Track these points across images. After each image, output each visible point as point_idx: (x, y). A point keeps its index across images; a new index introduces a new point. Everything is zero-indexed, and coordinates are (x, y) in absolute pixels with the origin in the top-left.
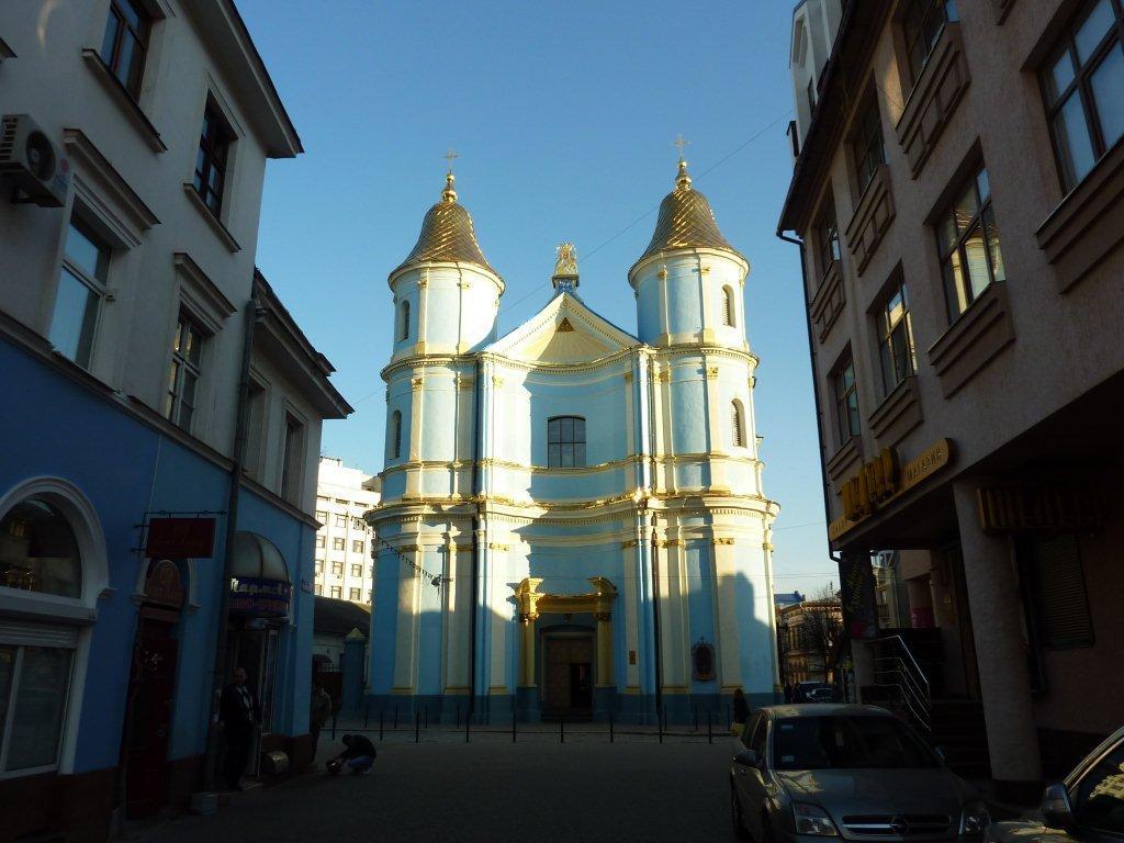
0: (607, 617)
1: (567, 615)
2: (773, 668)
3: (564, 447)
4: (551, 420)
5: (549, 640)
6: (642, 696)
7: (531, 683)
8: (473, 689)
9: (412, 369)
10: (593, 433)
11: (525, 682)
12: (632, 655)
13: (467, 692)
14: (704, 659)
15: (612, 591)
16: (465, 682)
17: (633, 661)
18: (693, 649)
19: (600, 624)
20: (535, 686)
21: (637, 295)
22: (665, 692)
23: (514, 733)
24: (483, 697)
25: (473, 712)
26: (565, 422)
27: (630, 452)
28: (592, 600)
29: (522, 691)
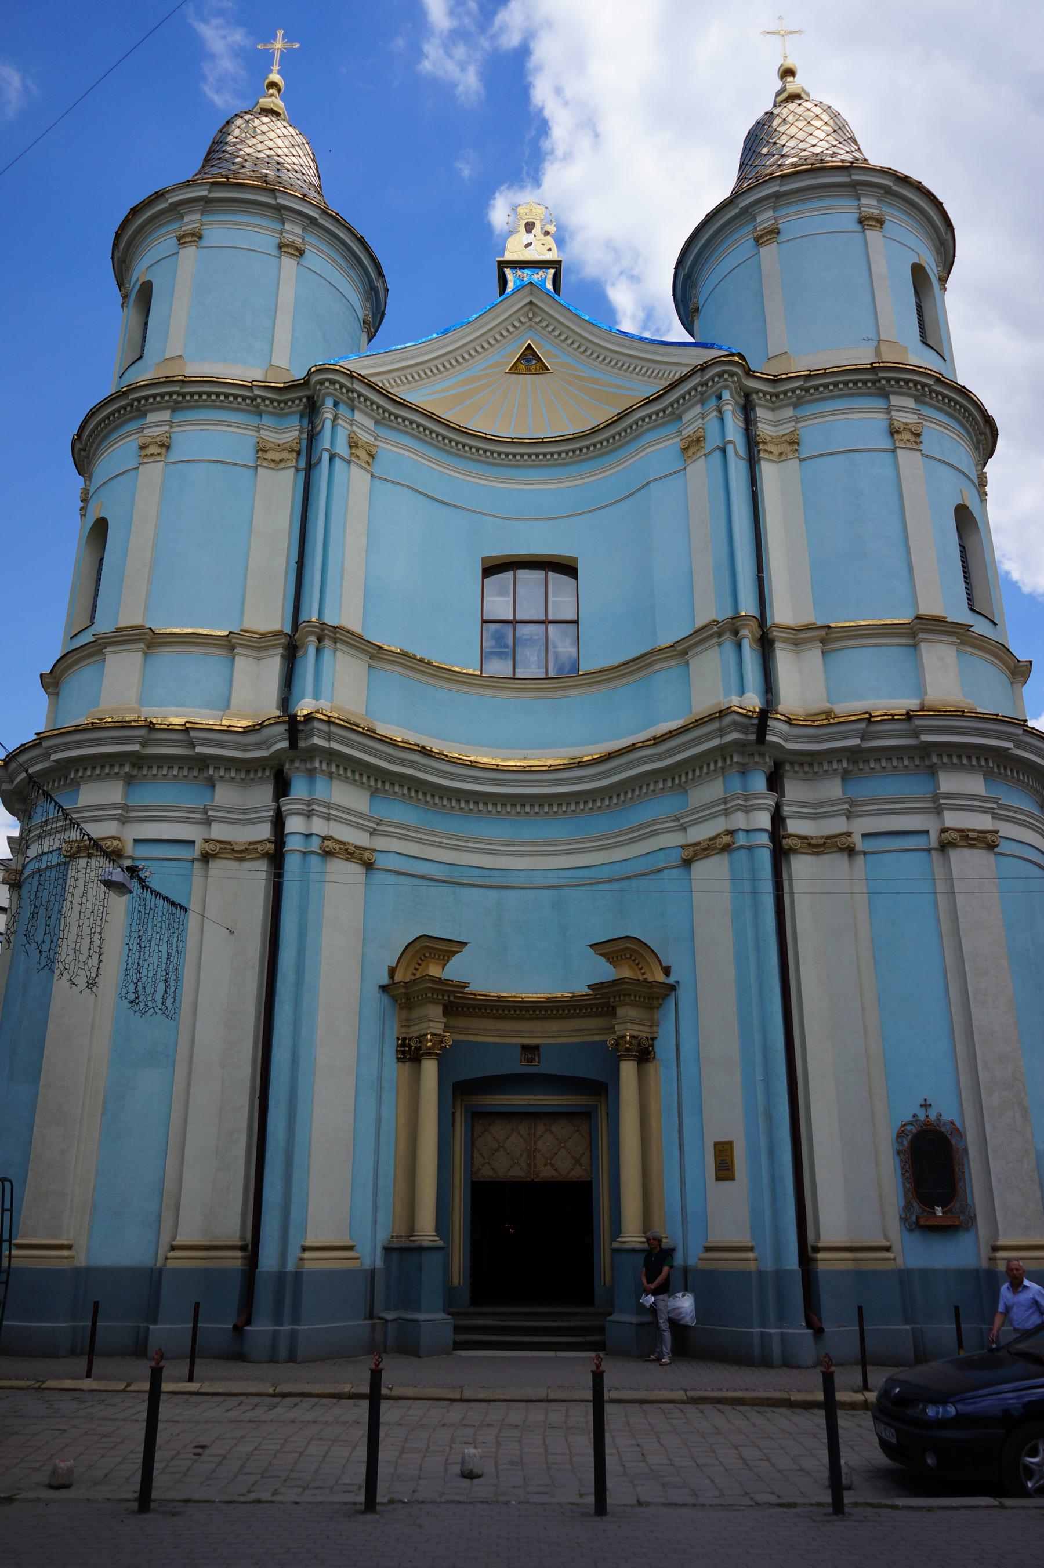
0: (644, 1054)
1: (525, 1048)
3: (524, 630)
4: (492, 568)
5: (477, 1116)
6: (760, 1274)
8: (252, 1249)
9: (144, 415)
11: (411, 1231)
13: (235, 1260)
15: (661, 977)
16: (230, 1226)
17: (724, 1170)
18: (901, 1134)
19: (628, 1069)
20: (440, 1243)
22: (825, 1262)
23: (375, 1398)
24: (281, 1276)
25: (248, 1322)
26: (524, 575)
27: (710, 610)
28: (603, 1001)
29: (402, 1253)
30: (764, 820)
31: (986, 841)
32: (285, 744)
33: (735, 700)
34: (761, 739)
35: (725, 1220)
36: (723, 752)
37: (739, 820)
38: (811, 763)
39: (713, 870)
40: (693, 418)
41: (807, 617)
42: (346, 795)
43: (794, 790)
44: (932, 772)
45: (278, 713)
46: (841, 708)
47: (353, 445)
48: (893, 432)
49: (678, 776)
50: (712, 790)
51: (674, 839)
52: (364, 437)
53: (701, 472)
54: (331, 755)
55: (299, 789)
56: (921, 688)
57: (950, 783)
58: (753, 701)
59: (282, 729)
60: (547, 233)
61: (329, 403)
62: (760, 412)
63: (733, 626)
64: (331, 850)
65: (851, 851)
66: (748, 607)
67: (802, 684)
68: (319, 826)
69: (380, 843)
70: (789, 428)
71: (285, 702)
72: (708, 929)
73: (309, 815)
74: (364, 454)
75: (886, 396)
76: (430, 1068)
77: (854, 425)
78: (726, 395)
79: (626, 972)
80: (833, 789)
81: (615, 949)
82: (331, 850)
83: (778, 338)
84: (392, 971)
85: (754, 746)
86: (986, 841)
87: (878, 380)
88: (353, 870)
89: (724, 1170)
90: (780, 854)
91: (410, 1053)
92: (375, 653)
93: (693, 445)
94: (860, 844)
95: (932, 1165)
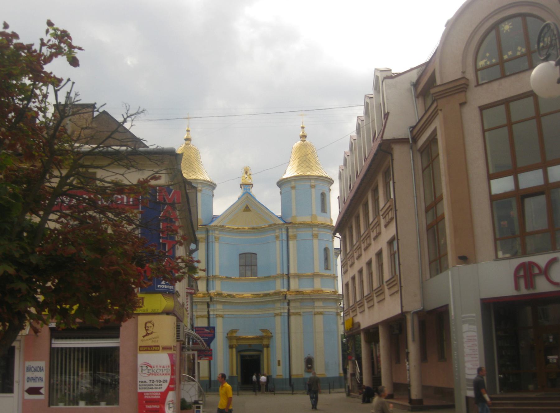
0: (268, 346)
2: (339, 366)
3: (247, 268)
7: (235, 374)
10: (261, 261)
12: (279, 362)
13: (208, 379)
14: (309, 362)
17: (279, 364)
19: (265, 349)
21: (281, 193)
22: (293, 377)
24: (214, 381)
27: (279, 272)
28: (261, 338)
30: (286, 311)
31: (321, 313)
32: (209, 300)
33: (282, 290)
34: (285, 299)
35: (279, 372)
36: (280, 300)
37: (282, 311)
38: (294, 300)
39: (278, 319)
40: (278, 232)
41: (296, 272)
42: (219, 307)
43: (292, 304)
44: (314, 302)
45: (206, 292)
46: (300, 290)
47: (215, 238)
48: (313, 236)
49: (274, 302)
50: (278, 305)
51: (273, 312)
52: (217, 236)
53: (278, 243)
54: (217, 301)
55: (212, 308)
56: (313, 287)
57: (317, 304)
58: (285, 290)
59: (209, 298)
60: (250, 175)
61: (211, 232)
62: (290, 230)
63: (282, 276)
64: (217, 316)
65: (300, 315)
66: (286, 272)
67: (294, 285)
68: (215, 313)
69: (225, 313)
70: (295, 233)
71: (207, 290)
72: (278, 327)
73: (214, 311)
74: (217, 239)
75: (312, 228)
76: (234, 350)
77: (305, 234)
78: (283, 230)
79: (264, 334)
80: (298, 304)
81: (263, 331)
82: (217, 316)
83: (294, 213)
84: (227, 334)
85: (285, 298)
86: (321, 313)
87: (311, 226)
88: (221, 318)
89: (279, 364)
90: (289, 315)
91: (231, 347)
92: (221, 279)
93: (277, 237)
94: (302, 314)
95: (309, 362)
